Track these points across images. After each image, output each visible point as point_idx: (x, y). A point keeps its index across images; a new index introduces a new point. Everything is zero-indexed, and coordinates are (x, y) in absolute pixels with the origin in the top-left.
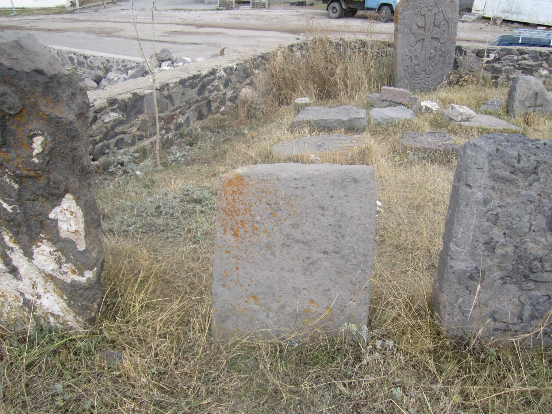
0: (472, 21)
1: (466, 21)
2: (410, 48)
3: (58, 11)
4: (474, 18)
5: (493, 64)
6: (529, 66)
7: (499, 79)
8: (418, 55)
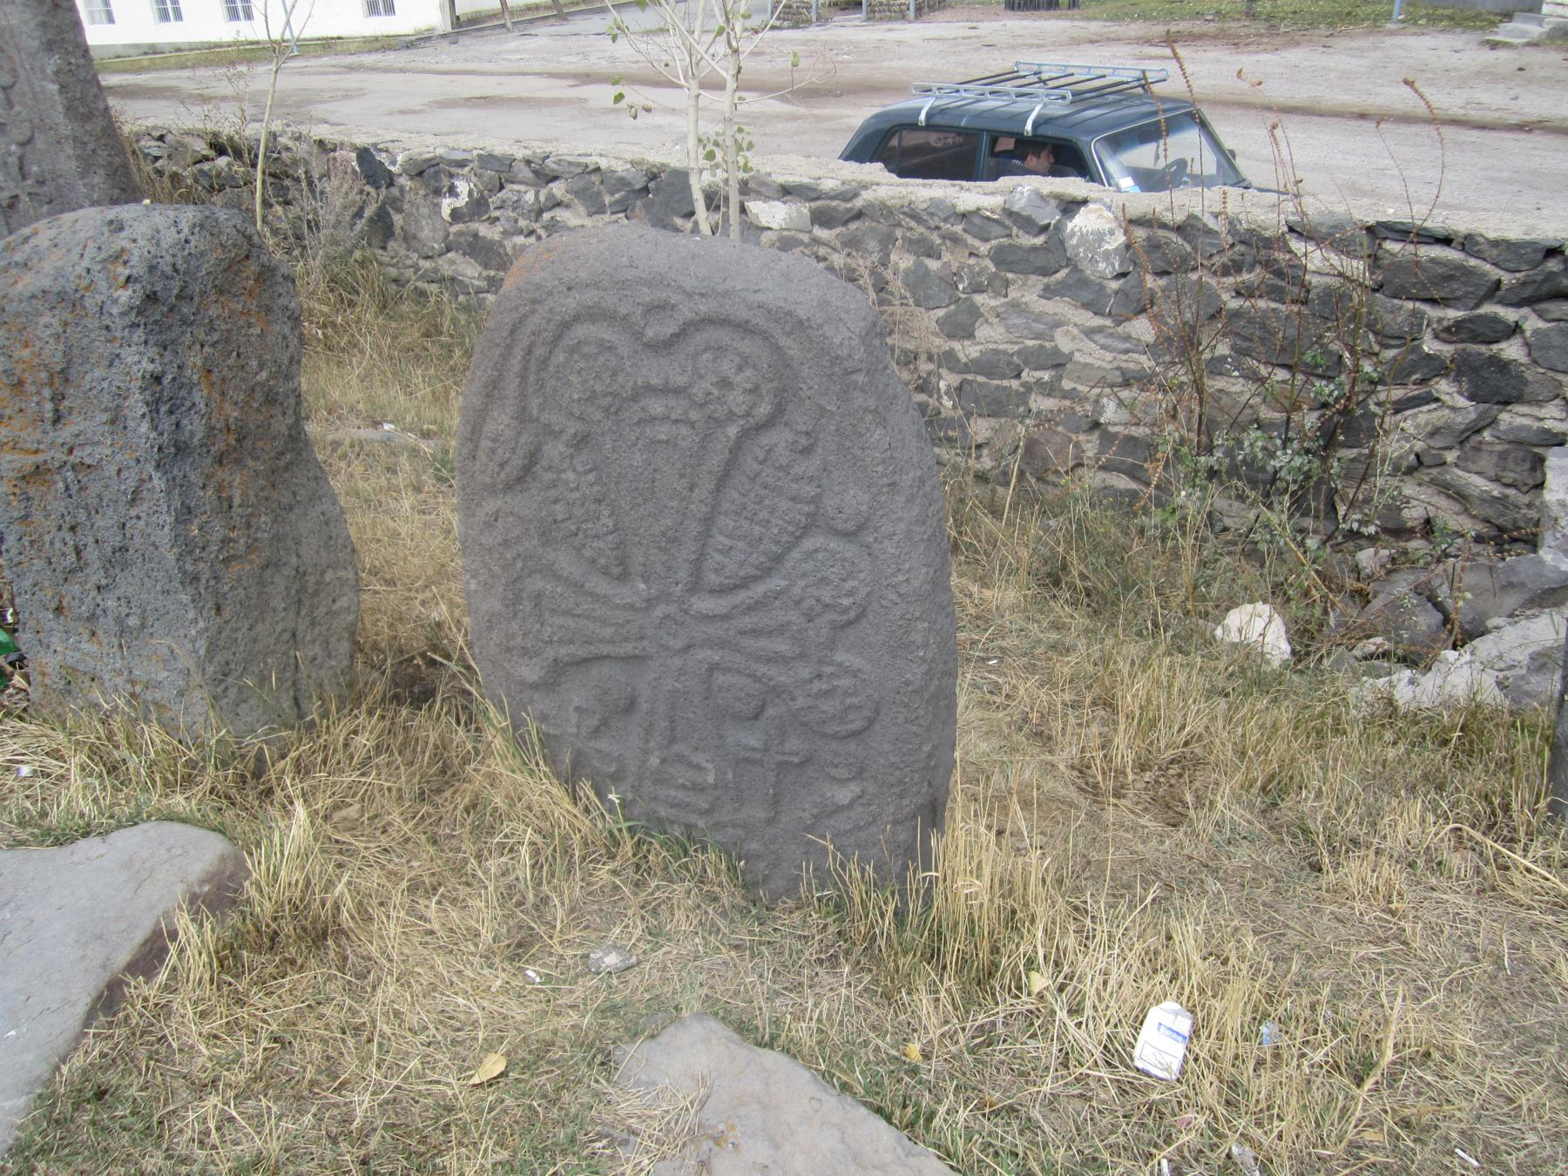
0: (1529, 44)
1: (1506, 45)
3: (378, 45)
4: (1535, 30)
5: (474, 226)
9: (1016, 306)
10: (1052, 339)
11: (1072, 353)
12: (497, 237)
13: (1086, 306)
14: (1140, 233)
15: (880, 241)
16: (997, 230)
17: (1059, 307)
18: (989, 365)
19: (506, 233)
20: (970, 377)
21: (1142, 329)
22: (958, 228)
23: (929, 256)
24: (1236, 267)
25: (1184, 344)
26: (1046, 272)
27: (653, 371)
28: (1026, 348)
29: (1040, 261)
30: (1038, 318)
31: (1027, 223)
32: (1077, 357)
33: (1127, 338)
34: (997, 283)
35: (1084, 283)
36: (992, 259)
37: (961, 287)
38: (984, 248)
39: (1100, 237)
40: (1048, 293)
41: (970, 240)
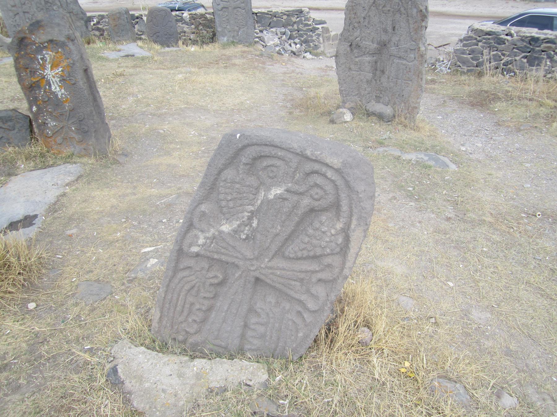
2: (12, 20)
5: (98, 26)
8: (19, 24)
13: (187, 25)
17: (184, 25)
19: (104, 26)
21: (193, 26)
24: (201, 18)
25: (197, 27)
26: (181, 21)
27: (159, 13)
29: (180, 20)
30: (181, 27)
31: (178, 16)
35: (186, 22)
39: (187, 16)
40: (182, 24)
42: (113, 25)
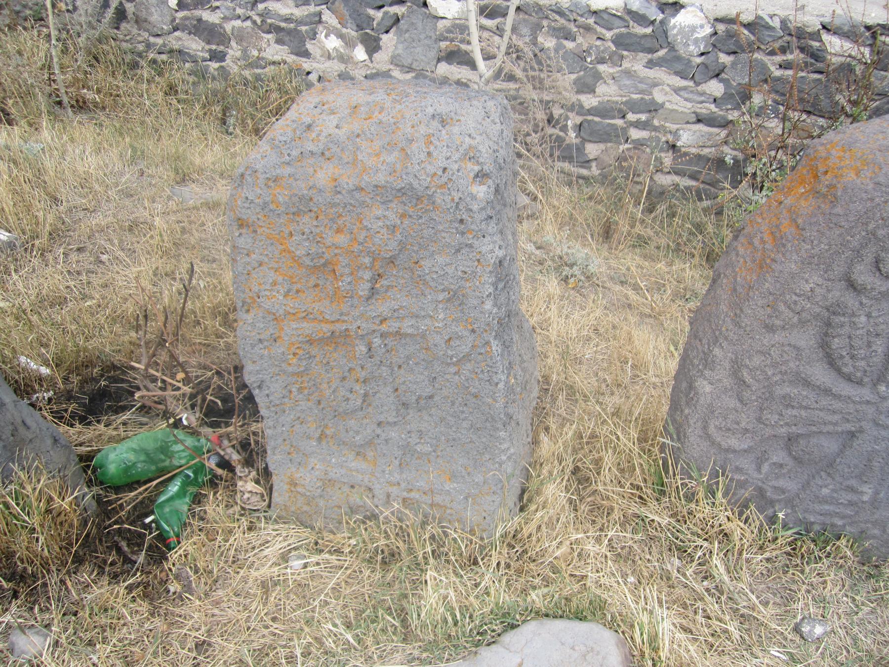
5: (198, 13)
6: (287, 20)
7: (228, 61)
9: (628, 73)
10: (651, 94)
11: (664, 103)
12: (217, 22)
13: (677, 73)
14: (721, 27)
15: (531, 29)
16: (617, 22)
18: (603, 111)
19: (225, 19)
20: (590, 118)
21: (715, 88)
22: (591, 21)
23: (566, 39)
24: (783, 50)
28: (631, 99)
29: (648, 44)
31: (640, 19)
32: (667, 105)
33: (703, 94)
34: (615, 58)
35: (678, 58)
36: (613, 42)
37: (589, 60)
38: (608, 35)
39: (693, 29)
40: (650, 64)
41: (599, 29)
42: (293, 329)
